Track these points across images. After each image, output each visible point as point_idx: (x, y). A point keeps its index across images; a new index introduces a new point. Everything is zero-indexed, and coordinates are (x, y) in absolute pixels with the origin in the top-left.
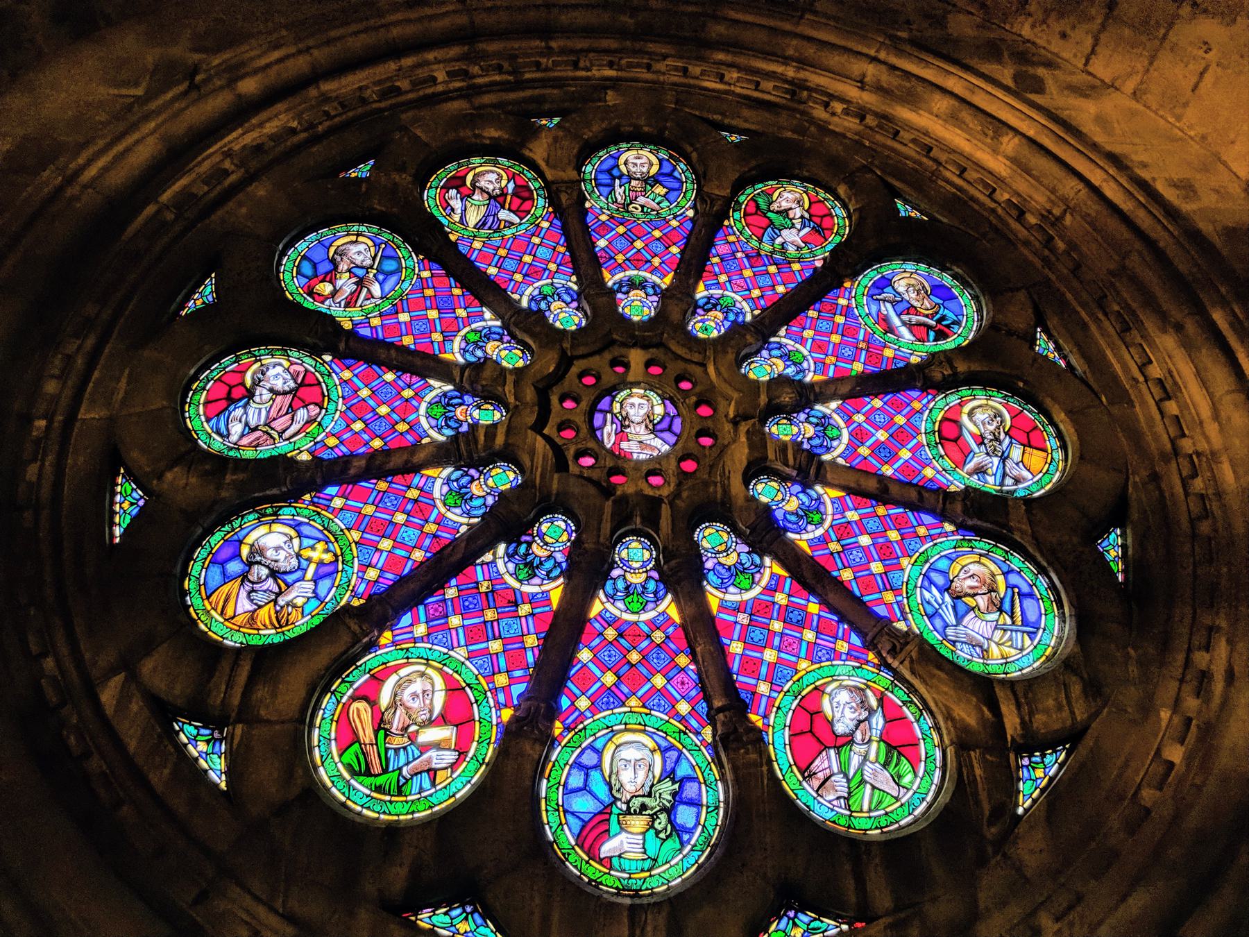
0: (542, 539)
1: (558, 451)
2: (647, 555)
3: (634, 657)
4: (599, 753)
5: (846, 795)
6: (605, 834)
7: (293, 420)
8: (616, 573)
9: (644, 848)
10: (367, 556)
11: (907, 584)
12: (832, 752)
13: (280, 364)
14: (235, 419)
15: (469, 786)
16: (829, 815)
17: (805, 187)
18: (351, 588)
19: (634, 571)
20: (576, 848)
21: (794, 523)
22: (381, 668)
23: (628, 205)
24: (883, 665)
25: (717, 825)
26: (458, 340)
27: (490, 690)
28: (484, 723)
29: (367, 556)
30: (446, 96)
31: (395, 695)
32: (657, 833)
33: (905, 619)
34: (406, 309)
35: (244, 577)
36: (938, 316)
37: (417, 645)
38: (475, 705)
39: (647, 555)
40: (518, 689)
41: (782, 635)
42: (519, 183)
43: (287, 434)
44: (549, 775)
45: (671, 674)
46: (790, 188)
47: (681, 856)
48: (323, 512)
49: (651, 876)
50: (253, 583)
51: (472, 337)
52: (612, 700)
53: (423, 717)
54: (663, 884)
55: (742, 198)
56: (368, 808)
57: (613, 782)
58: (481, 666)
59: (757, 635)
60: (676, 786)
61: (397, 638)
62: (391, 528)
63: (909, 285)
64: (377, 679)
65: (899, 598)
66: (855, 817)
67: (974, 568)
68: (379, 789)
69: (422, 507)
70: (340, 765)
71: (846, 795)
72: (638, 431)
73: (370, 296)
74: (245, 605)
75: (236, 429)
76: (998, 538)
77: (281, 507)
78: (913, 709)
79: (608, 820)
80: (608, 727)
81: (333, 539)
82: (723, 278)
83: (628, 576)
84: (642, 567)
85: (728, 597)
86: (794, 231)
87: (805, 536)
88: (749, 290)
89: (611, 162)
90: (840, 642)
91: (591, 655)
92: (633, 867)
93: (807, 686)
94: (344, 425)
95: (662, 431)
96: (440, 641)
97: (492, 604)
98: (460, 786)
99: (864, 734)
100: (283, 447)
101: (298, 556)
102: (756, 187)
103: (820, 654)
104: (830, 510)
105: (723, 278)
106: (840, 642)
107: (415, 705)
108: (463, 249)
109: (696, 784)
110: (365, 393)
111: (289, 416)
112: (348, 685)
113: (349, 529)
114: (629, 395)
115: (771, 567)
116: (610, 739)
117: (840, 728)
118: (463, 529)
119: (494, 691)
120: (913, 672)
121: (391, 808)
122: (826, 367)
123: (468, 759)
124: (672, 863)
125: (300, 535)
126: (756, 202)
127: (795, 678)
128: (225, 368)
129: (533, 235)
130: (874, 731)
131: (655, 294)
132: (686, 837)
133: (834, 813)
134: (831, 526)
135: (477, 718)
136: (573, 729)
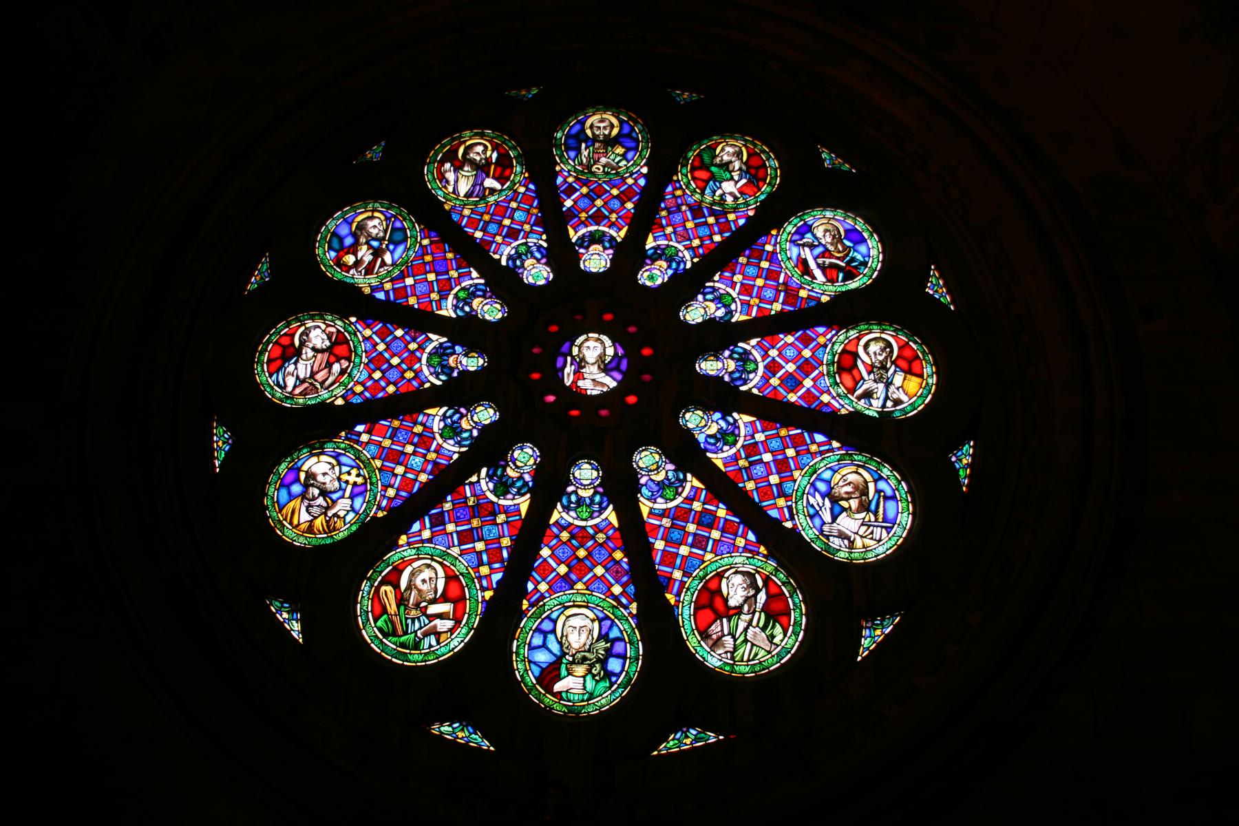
0: (515, 464)
3: (582, 553)
4: (555, 622)
5: (732, 650)
6: (558, 678)
7: (330, 372)
8: (570, 489)
10: (387, 479)
11: (797, 491)
12: (725, 620)
13: (319, 327)
14: (289, 373)
15: (463, 644)
16: (719, 663)
18: (377, 503)
19: (585, 487)
20: (538, 686)
23: (592, 166)
25: (636, 671)
26: (451, 297)
27: (476, 577)
28: (473, 600)
33: (792, 518)
34: (411, 274)
35: (303, 496)
37: (425, 545)
39: (595, 474)
40: (497, 577)
41: (695, 535)
42: (502, 151)
43: (328, 383)
44: (519, 637)
45: (609, 566)
46: (732, 142)
47: (610, 692)
48: (355, 446)
49: (588, 704)
51: (462, 295)
52: (564, 584)
53: (430, 596)
54: (596, 710)
56: (396, 658)
57: (564, 641)
58: (470, 560)
59: (676, 535)
60: (608, 645)
62: (402, 458)
63: (826, 231)
64: (398, 571)
65: (789, 503)
66: (737, 665)
67: (852, 478)
69: (424, 441)
70: (375, 629)
71: (732, 650)
72: (592, 371)
73: (383, 264)
74: (305, 517)
75: (291, 382)
77: (325, 443)
78: (789, 587)
80: (560, 604)
81: (362, 466)
82: (669, 230)
85: (656, 506)
86: (732, 183)
87: (721, 455)
88: (690, 240)
89: (577, 128)
90: (738, 539)
91: (549, 552)
92: (576, 698)
93: (711, 572)
95: (612, 370)
96: (441, 542)
100: (324, 395)
101: (339, 479)
102: (702, 143)
103: (722, 548)
104: (742, 434)
105: (669, 230)
106: (738, 539)
107: (425, 587)
109: (622, 644)
111: (326, 371)
114: (586, 340)
115: (691, 481)
116: (562, 613)
118: (456, 456)
119: (480, 578)
121: (410, 657)
122: (750, 307)
123: (462, 626)
125: (340, 464)
127: (701, 567)
128: (279, 333)
129: (512, 200)
130: (758, 604)
131: (611, 247)
132: (614, 679)
134: (743, 446)
136: (536, 606)
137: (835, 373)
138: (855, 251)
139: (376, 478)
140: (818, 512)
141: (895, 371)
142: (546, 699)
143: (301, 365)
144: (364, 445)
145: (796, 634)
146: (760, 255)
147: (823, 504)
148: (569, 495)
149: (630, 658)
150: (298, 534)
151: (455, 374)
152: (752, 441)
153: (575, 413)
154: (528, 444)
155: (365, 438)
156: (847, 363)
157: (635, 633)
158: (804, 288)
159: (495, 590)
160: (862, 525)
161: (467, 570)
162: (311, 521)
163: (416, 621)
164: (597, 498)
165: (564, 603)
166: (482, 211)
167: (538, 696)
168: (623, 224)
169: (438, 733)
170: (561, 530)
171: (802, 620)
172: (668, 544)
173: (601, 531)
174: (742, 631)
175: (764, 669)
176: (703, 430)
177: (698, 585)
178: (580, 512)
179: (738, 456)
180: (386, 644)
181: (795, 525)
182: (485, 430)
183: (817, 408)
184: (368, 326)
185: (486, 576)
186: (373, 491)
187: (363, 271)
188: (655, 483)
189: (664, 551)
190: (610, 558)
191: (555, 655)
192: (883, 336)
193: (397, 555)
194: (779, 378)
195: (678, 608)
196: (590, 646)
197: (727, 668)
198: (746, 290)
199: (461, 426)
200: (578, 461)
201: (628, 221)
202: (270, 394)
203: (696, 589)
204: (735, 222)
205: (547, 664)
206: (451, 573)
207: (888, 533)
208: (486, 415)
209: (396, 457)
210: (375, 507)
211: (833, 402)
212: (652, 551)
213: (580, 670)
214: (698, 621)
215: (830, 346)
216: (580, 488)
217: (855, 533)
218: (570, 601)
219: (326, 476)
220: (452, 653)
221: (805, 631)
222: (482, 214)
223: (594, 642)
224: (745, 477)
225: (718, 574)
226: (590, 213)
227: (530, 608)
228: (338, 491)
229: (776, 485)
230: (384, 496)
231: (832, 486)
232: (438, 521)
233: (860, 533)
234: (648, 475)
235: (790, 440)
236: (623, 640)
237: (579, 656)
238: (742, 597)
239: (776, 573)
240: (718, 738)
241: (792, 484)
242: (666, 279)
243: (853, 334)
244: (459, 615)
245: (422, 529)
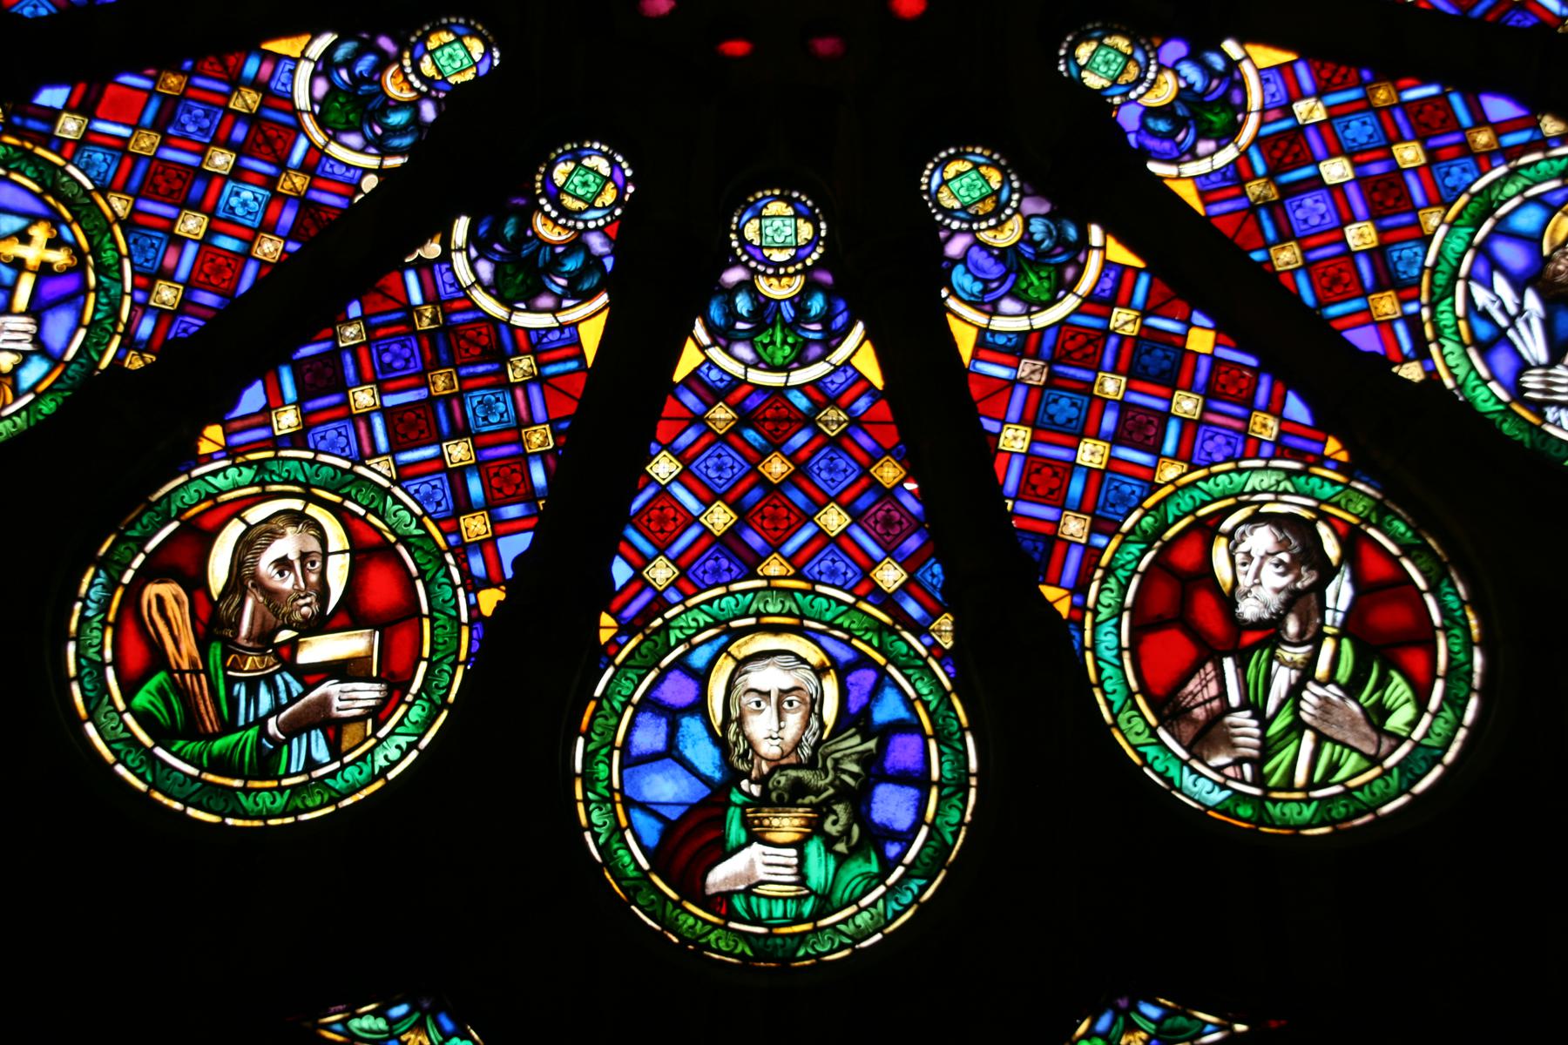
0: (557, 204)
2: (806, 231)
4: (702, 678)
5: (1255, 753)
8: (733, 276)
10: (151, 254)
12: (1229, 664)
15: (414, 755)
16: (1218, 796)
18: (121, 328)
22: (203, 506)
25: (961, 823)
27: (451, 549)
32: (829, 842)
33: (1421, 353)
37: (283, 453)
38: (419, 584)
39: (806, 231)
40: (513, 546)
41: (1123, 406)
45: (862, 504)
47: (881, 889)
48: (40, 151)
49: (816, 930)
52: (725, 563)
53: (305, 610)
54: (842, 947)
57: (731, 737)
58: (428, 497)
59: (1064, 408)
60: (871, 744)
61: (238, 439)
64: (199, 536)
65: (1412, 308)
66: (1275, 801)
68: (221, 764)
70: (128, 717)
78: (1427, 563)
81: (67, 214)
83: (762, 284)
85: (999, 324)
87: (1191, 169)
90: (1258, 418)
92: (778, 910)
93: (1178, 519)
96: (333, 444)
98: (394, 754)
103: (1209, 446)
104: (1255, 99)
106: (1258, 418)
107: (287, 584)
109: (914, 742)
115: (1103, 248)
116: (724, 649)
117: (1249, 609)
118: (370, 183)
119: (462, 551)
121: (247, 803)
123: (409, 698)
127: (1149, 503)
130: (1329, 615)
132: (893, 850)
133: (1227, 793)
134: (1257, 140)
135: (425, 610)
136: (641, 629)
139: (117, 249)
140: (1502, 332)
142: (682, 917)
144: (67, 153)
145: (1455, 702)
149: (940, 785)
153: (737, 47)
154: (596, 146)
155: (70, 126)
157: (952, 708)
159: (511, 587)
161: (421, 525)
163: (263, 690)
164: (817, 304)
165: (727, 621)
167: (657, 908)
169: (339, 1038)
170: (709, 400)
171: (1470, 661)
172: (1043, 436)
173: (833, 401)
174: (1283, 695)
175: (1360, 814)
176: (1133, 95)
177: (1139, 559)
178: (765, 346)
179: (1246, 173)
180: (165, 764)
181: (1432, 375)
182: (455, 99)
183: (1491, 17)
185: (480, 546)
186: (107, 290)
188: (990, 255)
189: (1028, 456)
190: (864, 482)
193: (193, 487)
195: (1082, 630)
196: (815, 748)
197: (1245, 811)
199: (382, 92)
200: (753, 194)
203: (1135, 571)
205: (681, 810)
209: (178, 185)
210: (117, 340)
212: (993, 458)
213: (787, 825)
214: (1144, 664)
216: (764, 274)
218: (746, 615)
220: (379, 784)
221: (1484, 693)
223: (825, 736)
224: (1270, 234)
225: (1199, 522)
227: (624, 639)
229: (1368, 253)
230: (141, 308)
231: (1546, 251)
234: (970, 231)
235: (1406, 116)
237: (783, 780)
238: (1278, 591)
239: (1380, 518)
240: (1230, 1028)
241: (1419, 250)
244: (399, 664)
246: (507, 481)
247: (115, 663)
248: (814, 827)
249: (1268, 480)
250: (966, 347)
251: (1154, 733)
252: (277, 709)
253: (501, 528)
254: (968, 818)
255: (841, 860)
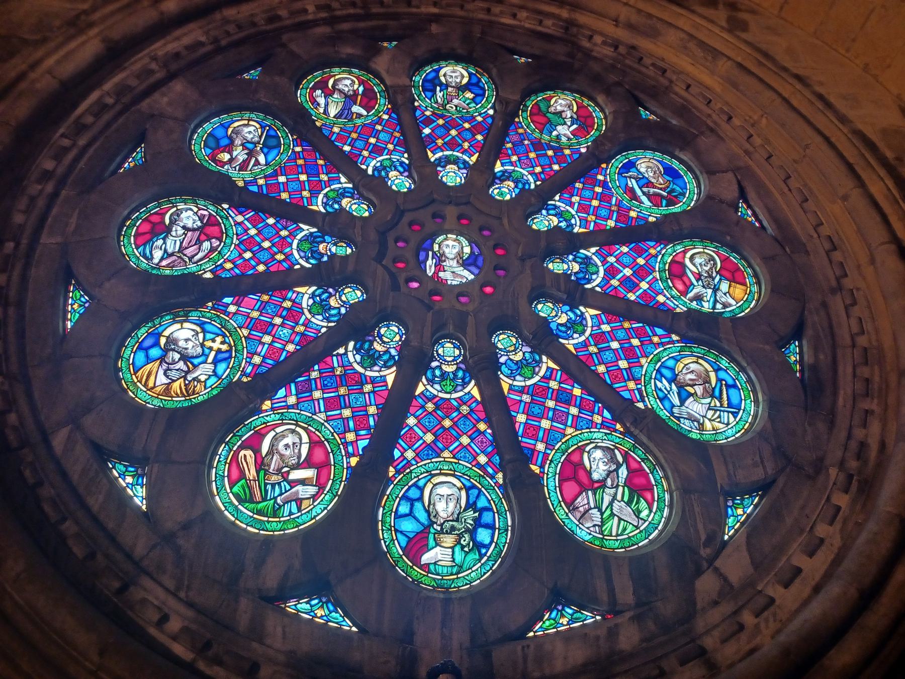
0: (381, 339)
1: (393, 276)
3: (447, 423)
4: (422, 490)
5: (600, 524)
6: (426, 548)
7: (200, 249)
9: (452, 558)
10: (253, 347)
11: (645, 375)
12: (590, 493)
13: (192, 210)
14: (157, 247)
15: (326, 511)
16: (587, 538)
17: (574, 96)
19: (448, 363)
20: (404, 557)
21: (564, 332)
24: (627, 433)
25: (506, 542)
26: (321, 196)
27: (342, 444)
28: (338, 466)
29: (253, 347)
30: (315, 23)
31: (273, 446)
32: (463, 547)
33: (643, 401)
34: (283, 173)
35: (162, 359)
36: (669, 189)
37: (289, 411)
38: (331, 454)
39: (457, 352)
40: (362, 444)
42: (369, 87)
45: (474, 436)
47: (480, 564)
49: (458, 578)
50: (169, 364)
51: (331, 195)
52: (430, 452)
53: (293, 462)
54: (467, 584)
55: (528, 103)
56: (251, 526)
57: (431, 510)
58: (336, 426)
59: (536, 410)
60: (477, 514)
61: (275, 405)
62: (270, 328)
63: (648, 167)
64: (259, 436)
65: (639, 386)
66: (606, 540)
67: (693, 366)
68: (259, 513)
69: (293, 314)
70: (231, 495)
71: (600, 524)
72: (451, 264)
73: (257, 163)
74: (162, 379)
75: (158, 255)
76: (711, 346)
77: (191, 311)
79: (428, 537)
81: (228, 335)
83: (444, 367)
84: (453, 361)
86: (566, 127)
87: (572, 342)
89: (433, 75)
91: (415, 421)
92: (445, 571)
93: (572, 446)
94: (237, 254)
95: (470, 265)
96: (306, 408)
97: (344, 383)
98: (319, 511)
99: (613, 481)
100: (193, 268)
101: (202, 345)
102: (539, 95)
103: (581, 424)
104: (590, 324)
105: (514, 158)
107: (288, 453)
108: (326, 132)
109: (491, 513)
110: (253, 232)
112: (238, 438)
113: (240, 328)
114: (446, 239)
116: (429, 480)
117: (596, 476)
118: (324, 330)
119: (346, 444)
120: (649, 438)
121: (268, 526)
123: (325, 492)
124: (473, 569)
125: (204, 331)
126: (538, 105)
127: (563, 440)
128: (150, 211)
129: (377, 123)
130: (620, 479)
131: (465, 168)
132: (483, 551)
134: (591, 335)
135: (332, 463)
137: (667, 279)
138: (674, 184)
140: (666, 395)
141: (721, 279)
142: (413, 572)
143: (169, 241)
144: (230, 316)
146: (595, 182)
147: (671, 388)
148: (434, 369)
150: (152, 396)
151: (325, 259)
152: (599, 331)
155: (232, 309)
156: (677, 271)
157: (502, 503)
158: (634, 210)
160: (709, 409)
161: (333, 435)
162: (169, 384)
163: (277, 487)
164: (460, 374)
166: (350, 130)
168: (474, 151)
170: (427, 401)
173: (465, 404)
175: (633, 545)
180: (241, 512)
182: (353, 307)
184: (240, 213)
185: (352, 443)
187: (237, 168)
191: (422, 524)
192: (706, 251)
193: (259, 420)
194: (618, 280)
195: (543, 480)
196: (458, 515)
198: (583, 208)
201: (479, 149)
202: (135, 264)
203: (559, 462)
204: (571, 156)
206: (316, 439)
207: (735, 417)
208: (353, 295)
210: (240, 372)
211: (667, 301)
213: (449, 540)
214: (564, 492)
215: (660, 256)
217: (703, 416)
218: (437, 469)
219: (190, 342)
220: (314, 521)
222: (350, 133)
226: (446, 140)
228: (201, 356)
232: (305, 389)
233: (709, 416)
236: (491, 510)
238: (604, 471)
242: (514, 196)
243: (679, 248)
244: (322, 481)
245: (287, 395)
246: (362, 423)
247: (228, 476)
248: (459, 542)
249: (600, 435)
250: (506, 390)
251: (567, 515)
252: (281, 494)
253: (359, 438)
254: (508, 541)
255: (467, 553)
